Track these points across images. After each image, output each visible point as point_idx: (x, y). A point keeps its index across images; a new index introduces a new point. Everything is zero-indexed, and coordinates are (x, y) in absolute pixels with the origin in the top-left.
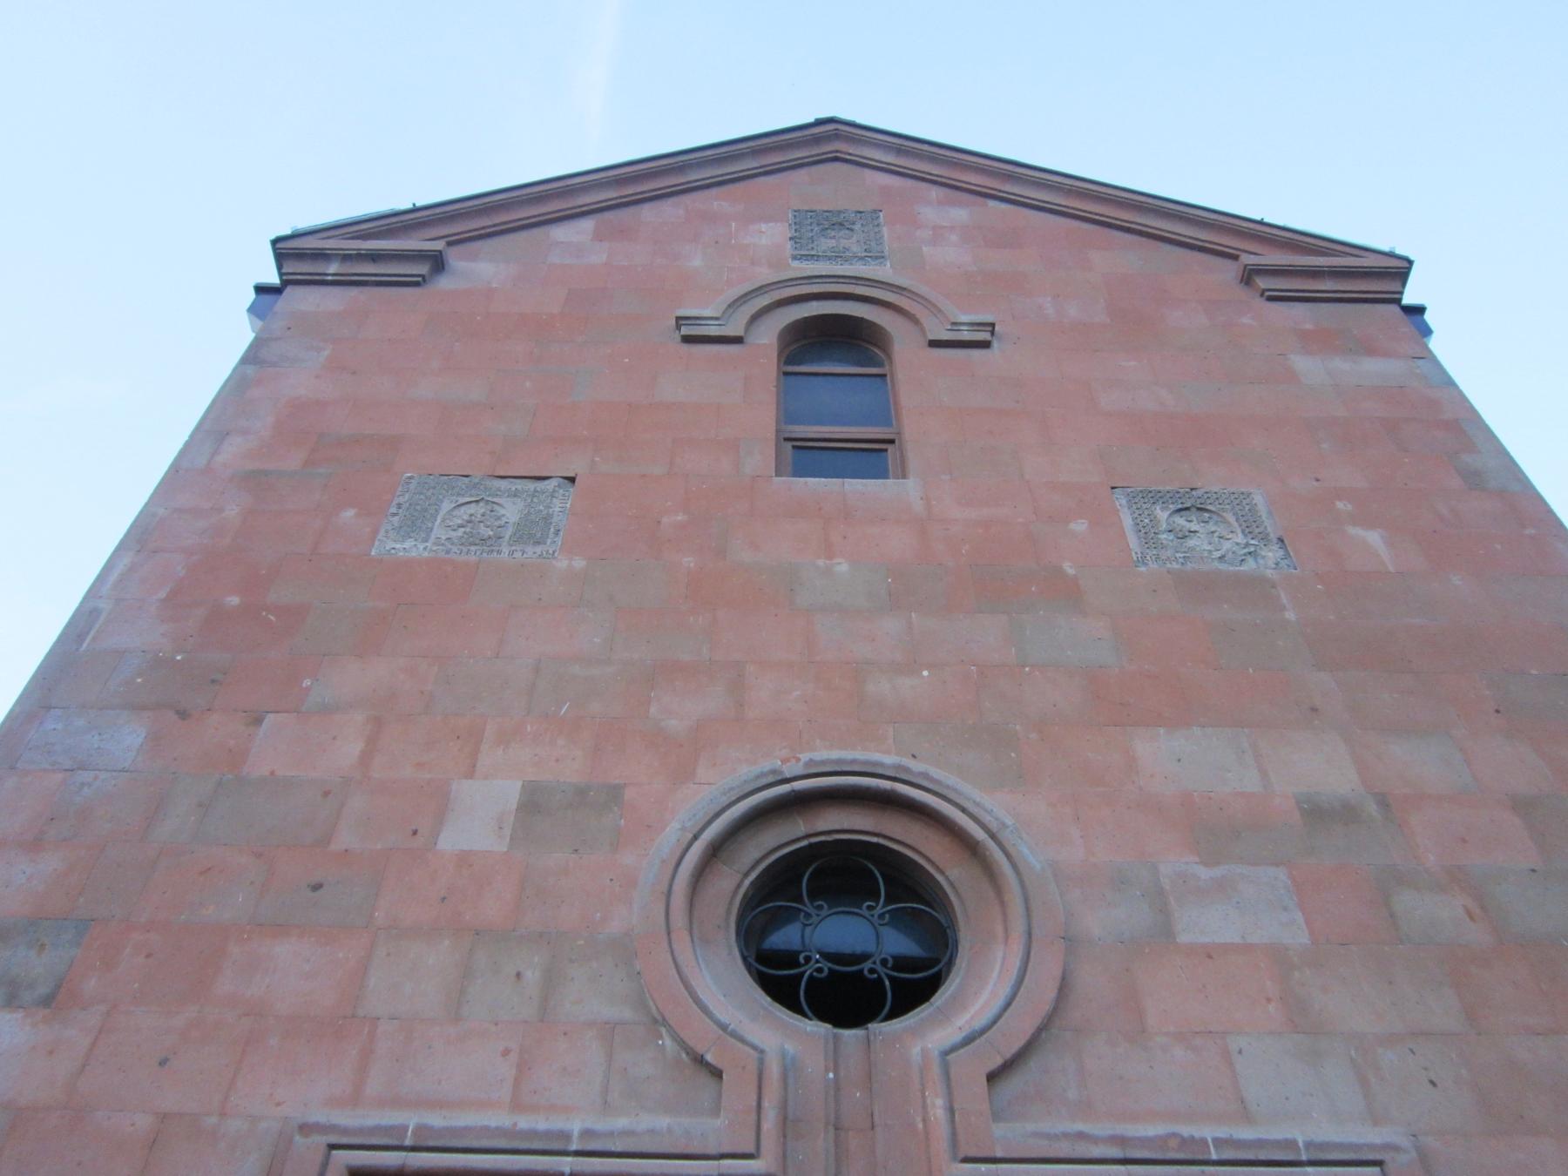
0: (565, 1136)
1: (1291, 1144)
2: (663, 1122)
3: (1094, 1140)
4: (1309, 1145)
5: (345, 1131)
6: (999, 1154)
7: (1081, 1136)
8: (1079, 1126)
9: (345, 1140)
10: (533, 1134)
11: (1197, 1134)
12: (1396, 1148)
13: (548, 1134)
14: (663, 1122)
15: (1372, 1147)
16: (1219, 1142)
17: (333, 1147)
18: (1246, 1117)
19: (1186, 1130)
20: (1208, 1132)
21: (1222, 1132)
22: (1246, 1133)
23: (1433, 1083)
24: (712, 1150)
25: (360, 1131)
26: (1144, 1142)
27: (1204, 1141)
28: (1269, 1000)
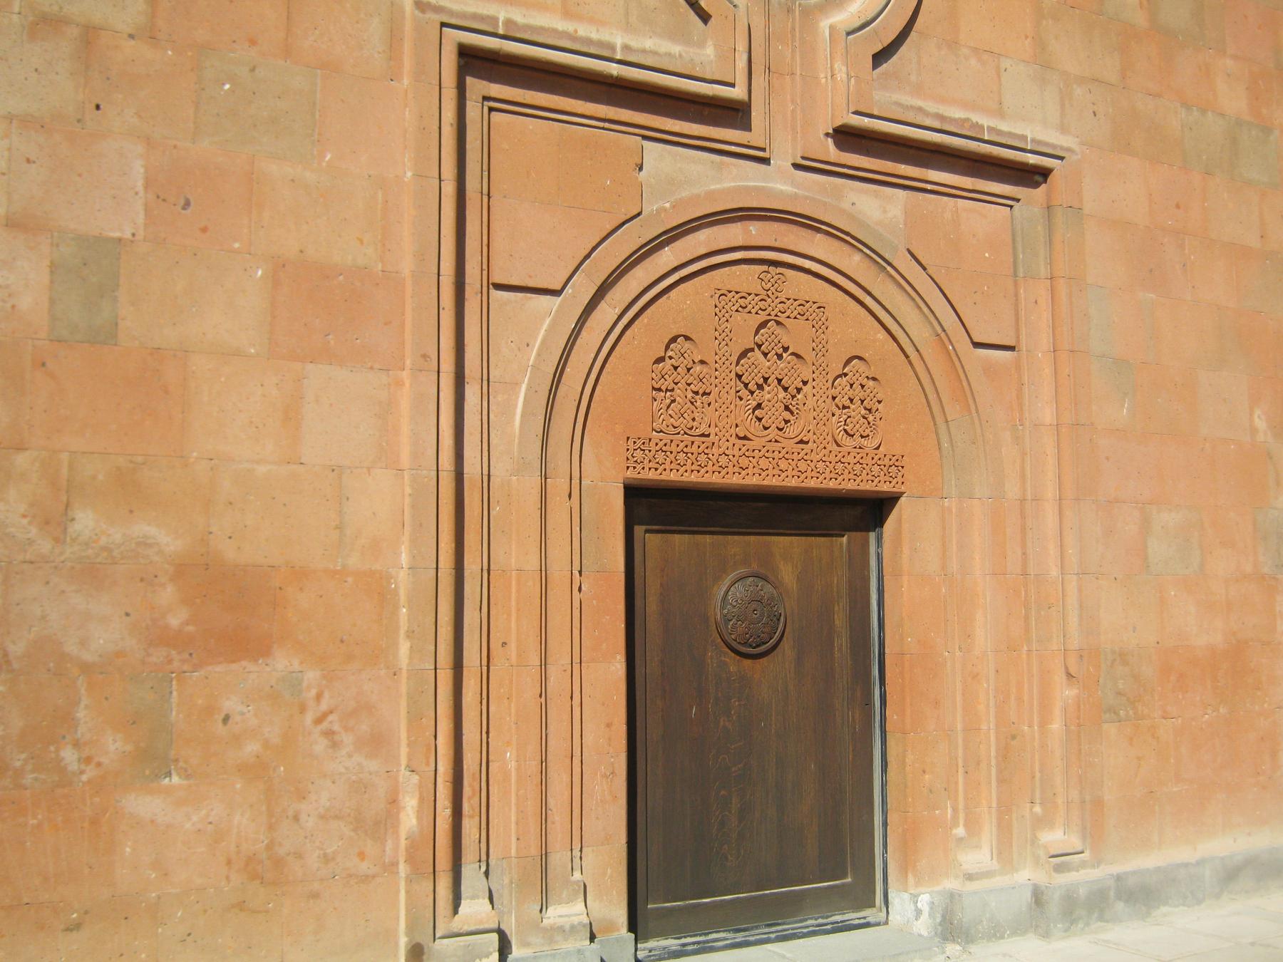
0: (612, 47)
1: (1024, 138)
2: (676, 49)
3: (927, 114)
4: (1033, 140)
5: (451, 13)
6: (876, 113)
7: (920, 109)
8: (920, 103)
9: (453, 21)
10: (589, 41)
11: (980, 122)
12: (1069, 150)
13: (600, 44)
14: (676, 49)
15: (1062, 148)
16: (991, 129)
17: (443, 25)
18: (1000, 113)
19: (976, 118)
20: (985, 121)
21: (992, 125)
22: (1004, 127)
23: (1095, 114)
24: (708, 77)
25: (464, 15)
26: (952, 120)
27: (982, 127)
28: (1027, 37)
